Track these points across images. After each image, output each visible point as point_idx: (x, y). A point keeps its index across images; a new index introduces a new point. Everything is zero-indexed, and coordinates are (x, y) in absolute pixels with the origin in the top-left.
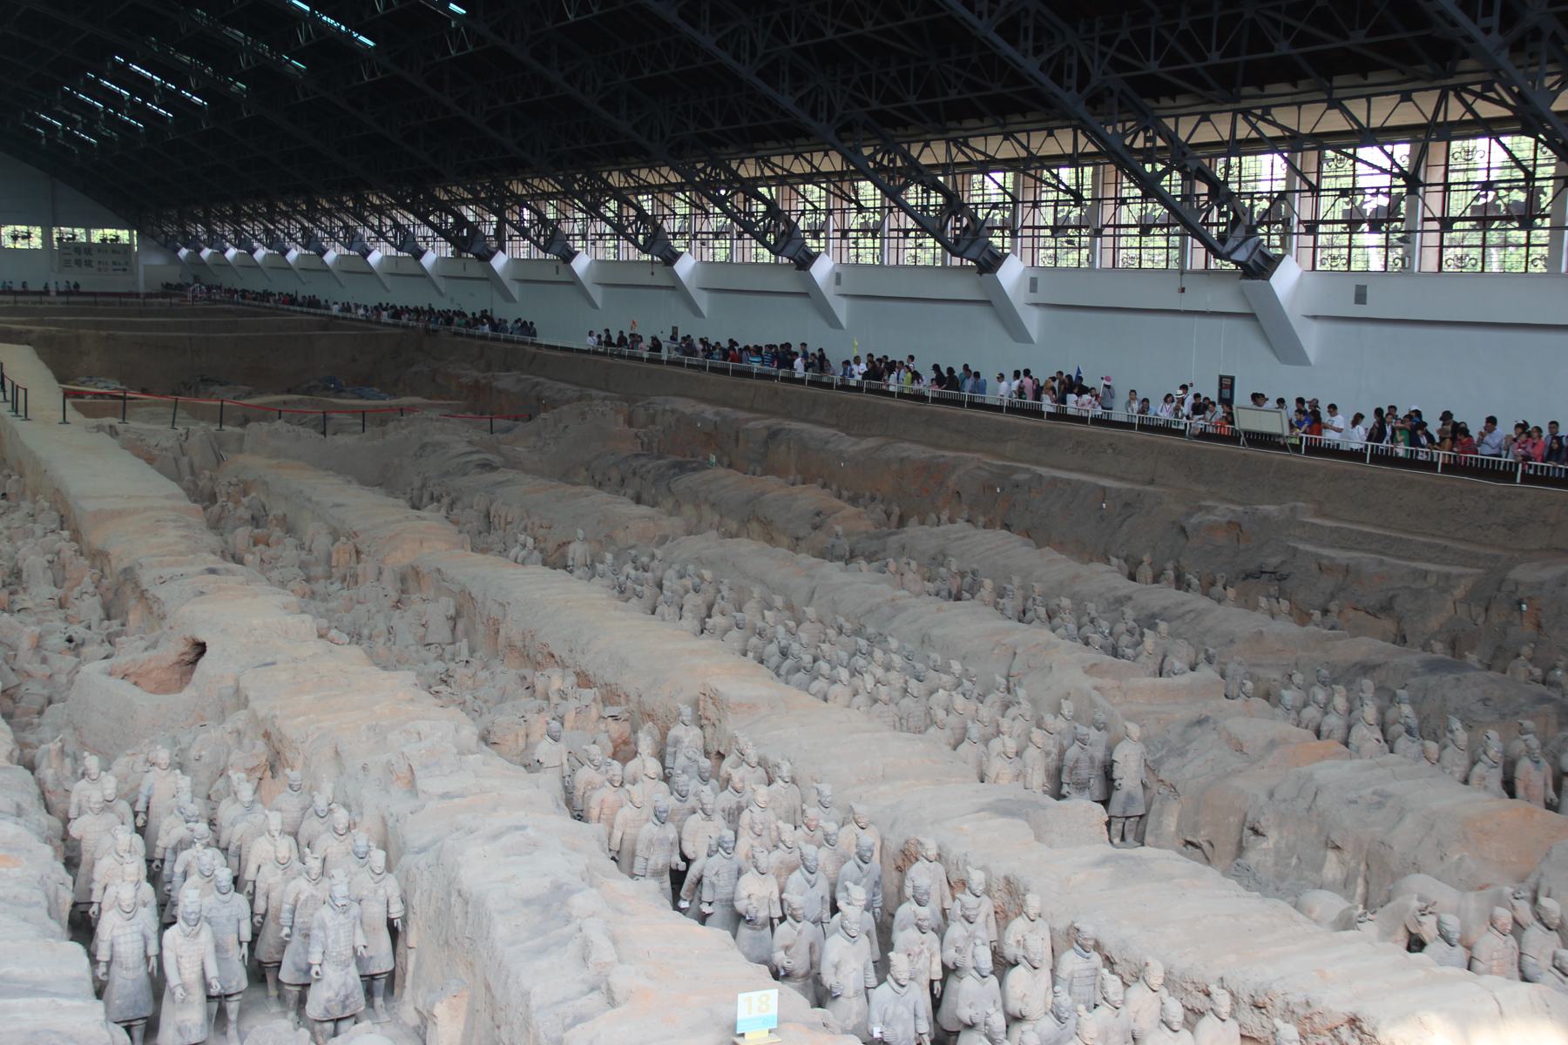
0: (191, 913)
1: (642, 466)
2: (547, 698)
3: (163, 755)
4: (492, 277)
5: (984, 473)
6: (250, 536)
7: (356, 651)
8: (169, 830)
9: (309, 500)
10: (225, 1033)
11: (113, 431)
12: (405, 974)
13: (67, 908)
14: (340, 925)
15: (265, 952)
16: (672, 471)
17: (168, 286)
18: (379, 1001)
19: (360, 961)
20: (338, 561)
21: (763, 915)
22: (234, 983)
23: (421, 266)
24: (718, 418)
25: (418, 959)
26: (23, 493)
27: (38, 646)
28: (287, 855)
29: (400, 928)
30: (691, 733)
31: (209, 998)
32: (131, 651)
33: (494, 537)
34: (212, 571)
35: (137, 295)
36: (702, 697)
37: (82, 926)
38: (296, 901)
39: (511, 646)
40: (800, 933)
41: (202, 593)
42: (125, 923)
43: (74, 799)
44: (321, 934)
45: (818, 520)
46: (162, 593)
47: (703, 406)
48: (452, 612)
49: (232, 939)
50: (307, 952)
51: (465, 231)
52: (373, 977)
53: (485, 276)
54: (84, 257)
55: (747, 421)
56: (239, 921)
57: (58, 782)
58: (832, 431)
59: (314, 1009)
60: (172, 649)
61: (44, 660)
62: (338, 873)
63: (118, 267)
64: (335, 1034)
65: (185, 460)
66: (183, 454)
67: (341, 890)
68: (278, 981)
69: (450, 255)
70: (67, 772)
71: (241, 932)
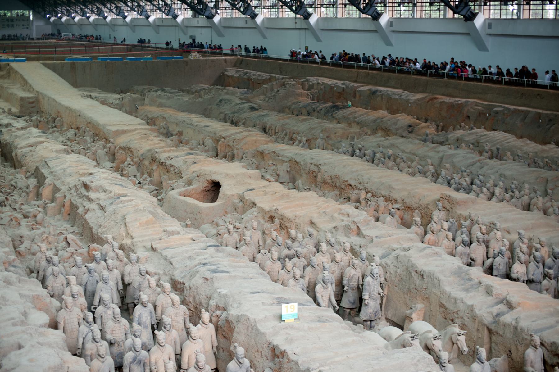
1: (318, 107)
2: (358, 201)
4: (213, 26)
5: (480, 108)
9: (191, 124)
11: (90, 97)
14: (375, 284)
16: (332, 110)
17: (46, 35)
20: (221, 149)
21: (522, 279)
23: (149, 22)
24: (344, 86)
25: (387, 299)
26: (62, 125)
30: (442, 214)
35: (33, 39)
36: (441, 199)
39: (325, 182)
40: (552, 284)
45: (411, 128)
47: (335, 81)
51: (201, 6)
53: (254, 26)
54: (10, 23)
55: (358, 87)
58: (400, 91)
60: (199, 186)
63: (24, 27)
69: (190, 17)
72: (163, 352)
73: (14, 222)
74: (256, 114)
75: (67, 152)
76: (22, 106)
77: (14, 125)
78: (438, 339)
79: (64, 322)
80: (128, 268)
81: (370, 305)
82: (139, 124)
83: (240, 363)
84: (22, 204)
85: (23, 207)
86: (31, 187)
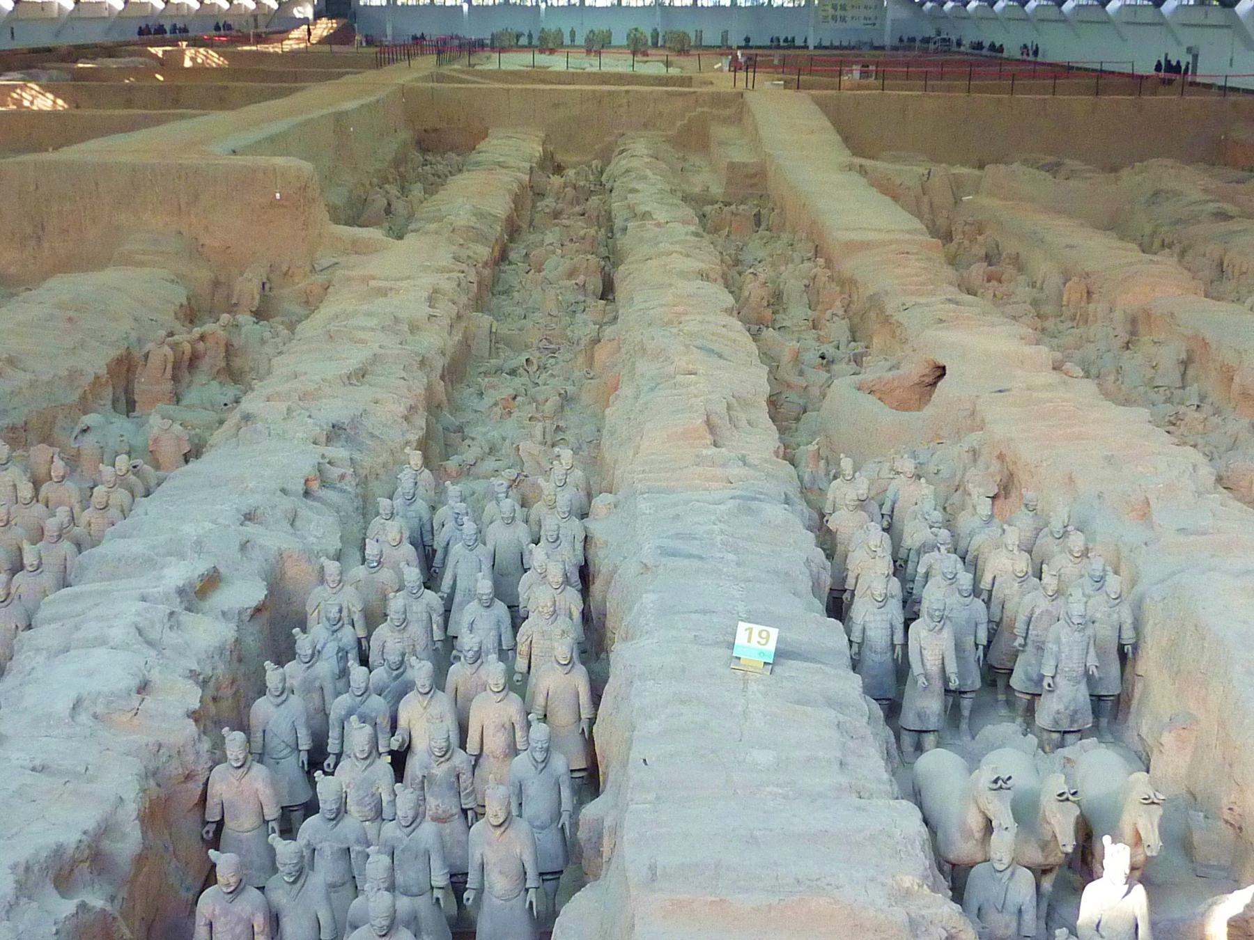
0: (936, 610)
3: (908, 466)
6: (984, 272)
7: (1090, 386)
8: (914, 534)
10: (958, 727)
11: (863, 171)
12: (1130, 700)
13: (827, 589)
15: (996, 659)
18: (1104, 722)
19: (1089, 678)
22: (969, 682)
26: (784, 224)
27: (797, 358)
28: (1025, 570)
29: (1130, 655)
31: (947, 691)
32: (874, 371)
33: (1229, 286)
34: (949, 300)
35: (882, 48)
37: (837, 606)
38: (1032, 615)
41: (941, 321)
42: (876, 610)
43: (830, 496)
44: (1055, 648)
46: (901, 317)
48: (1183, 356)
49: (970, 641)
50: (1040, 664)
52: (1100, 698)
54: (839, 13)
56: (976, 624)
57: (814, 481)
59: (1043, 718)
60: (914, 370)
61: (801, 373)
62: (1077, 594)
63: (868, 22)
64: (1062, 745)
65: (926, 199)
66: (924, 194)
67: (1077, 608)
68: (1008, 686)
70: (822, 473)
71: (978, 635)
72: (425, 708)
73: (498, 410)
74: (1233, 226)
75: (704, 276)
76: (730, 182)
77: (654, 217)
78: (1067, 799)
79: (319, 612)
80: (550, 525)
81: (1058, 692)
82: (909, 232)
83: (537, 762)
84: (552, 375)
85: (552, 381)
86: (583, 342)
